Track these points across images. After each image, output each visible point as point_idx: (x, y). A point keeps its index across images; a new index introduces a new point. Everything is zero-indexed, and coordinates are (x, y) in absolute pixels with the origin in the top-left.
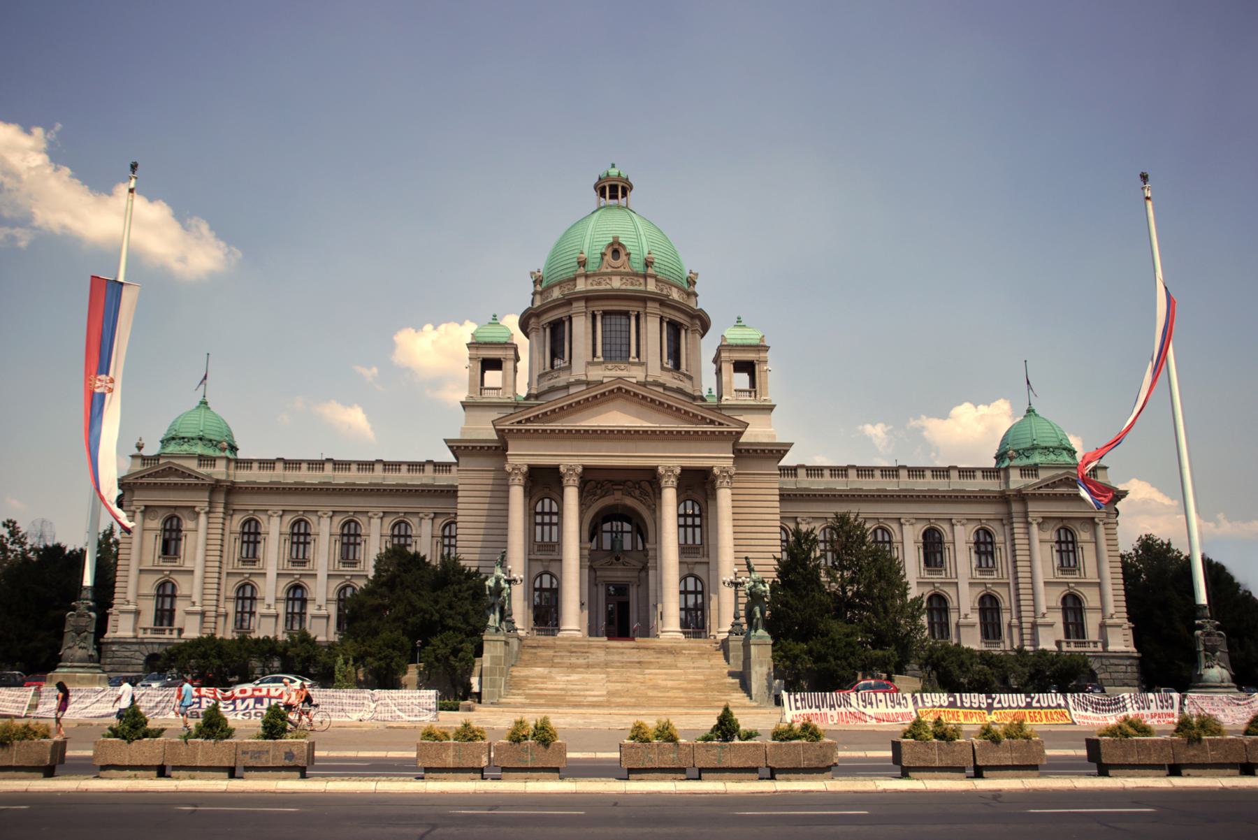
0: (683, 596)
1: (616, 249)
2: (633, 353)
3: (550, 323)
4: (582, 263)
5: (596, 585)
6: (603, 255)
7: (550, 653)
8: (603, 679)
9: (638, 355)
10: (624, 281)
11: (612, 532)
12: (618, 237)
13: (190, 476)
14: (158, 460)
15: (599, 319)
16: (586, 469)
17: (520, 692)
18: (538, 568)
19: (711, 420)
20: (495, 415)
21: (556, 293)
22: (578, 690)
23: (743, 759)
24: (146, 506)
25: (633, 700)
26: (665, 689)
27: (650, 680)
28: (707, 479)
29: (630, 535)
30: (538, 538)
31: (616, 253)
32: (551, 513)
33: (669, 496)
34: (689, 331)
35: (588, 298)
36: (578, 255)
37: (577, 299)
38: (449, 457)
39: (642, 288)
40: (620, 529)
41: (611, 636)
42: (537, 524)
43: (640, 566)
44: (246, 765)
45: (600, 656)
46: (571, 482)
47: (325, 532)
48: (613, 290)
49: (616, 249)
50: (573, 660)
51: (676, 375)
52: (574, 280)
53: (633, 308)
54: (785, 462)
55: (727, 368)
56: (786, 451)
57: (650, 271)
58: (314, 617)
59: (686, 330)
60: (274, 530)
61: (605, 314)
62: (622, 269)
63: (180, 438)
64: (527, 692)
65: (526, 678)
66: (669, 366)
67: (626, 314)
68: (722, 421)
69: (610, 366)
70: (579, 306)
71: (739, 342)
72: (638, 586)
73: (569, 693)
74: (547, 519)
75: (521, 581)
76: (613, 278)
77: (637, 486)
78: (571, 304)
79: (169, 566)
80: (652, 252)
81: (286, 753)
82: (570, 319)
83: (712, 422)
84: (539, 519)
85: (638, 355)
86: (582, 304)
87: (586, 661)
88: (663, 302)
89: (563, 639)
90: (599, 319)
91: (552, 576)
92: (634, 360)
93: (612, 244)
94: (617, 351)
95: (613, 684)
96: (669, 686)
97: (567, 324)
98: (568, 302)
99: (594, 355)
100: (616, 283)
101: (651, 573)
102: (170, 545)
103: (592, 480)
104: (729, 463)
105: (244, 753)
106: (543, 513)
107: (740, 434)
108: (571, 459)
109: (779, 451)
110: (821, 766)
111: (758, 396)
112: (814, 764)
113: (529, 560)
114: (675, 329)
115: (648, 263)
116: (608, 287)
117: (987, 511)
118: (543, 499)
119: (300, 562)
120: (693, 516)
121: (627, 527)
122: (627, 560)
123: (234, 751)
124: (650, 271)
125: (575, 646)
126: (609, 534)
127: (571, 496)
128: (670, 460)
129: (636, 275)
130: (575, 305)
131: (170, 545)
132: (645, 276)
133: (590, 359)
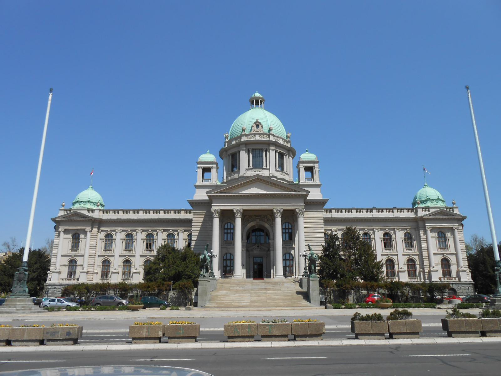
0: (284, 261)
1: (257, 124)
2: (265, 164)
3: (231, 154)
5: (249, 257)
6: (252, 126)
7: (229, 285)
8: (249, 296)
9: (266, 166)
10: (261, 136)
11: (256, 236)
12: (258, 120)
14: (71, 211)
16: (245, 211)
17: (214, 302)
18: (225, 251)
19: (294, 190)
20: (207, 190)
22: (239, 300)
23: (281, 331)
25: (261, 304)
26: (274, 299)
27: (269, 295)
28: (294, 214)
29: (263, 237)
30: (225, 239)
31: (257, 126)
32: (230, 229)
33: (279, 221)
34: (287, 156)
35: (246, 144)
36: (242, 127)
38: (190, 208)
39: (268, 139)
40: (259, 234)
41: (255, 278)
42: (225, 233)
43: (267, 249)
44: (48, 339)
45: (249, 287)
46: (238, 216)
47: (140, 237)
48: (256, 140)
49: (257, 124)
50: (238, 288)
51: (282, 173)
52: (240, 137)
53: (264, 147)
54: (326, 207)
55: (302, 170)
56: (326, 202)
57: (271, 132)
58: (134, 273)
59: (286, 156)
61: (253, 150)
62: (260, 132)
64: (217, 301)
65: (217, 296)
66: (279, 170)
68: (298, 190)
69: (255, 170)
71: (307, 160)
72: (267, 258)
73: (234, 302)
74: (229, 231)
75: (217, 256)
76: (256, 135)
77: (266, 217)
78: (240, 146)
79: (74, 253)
80: (272, 125)
81: (67, 332)
83: (295, 191)
84: (226, 231)
85: (266, 166)
86: (244, 146)
87: (243, 288)
88: (276, 144)
89: (234, 280)
90: (251, 151)
91: (231, 254)
92: (265, 168)
93: (255, 123)
94: (257, 163)
95: (253, 298)
96: (276, 298)
97: (238, 154)
100: (258, 138)
101: (271, 252)
102: (75, 245)
103: (247, 216)
104: (303, 207)
105: (47, 333)
106: (227, 229)
107: (307, 196)
108: (237, 207)
109: (323, 202)
110: (317, 333)
111: (315, 181)
112: (314, 333)
113: (221, 248)
114: (281, 156)
115: (270, 130)
116: (254, 139)
118: (227, 223)
120: (289, 229)
121: (262, 234)
122: (262, 247)
123: (42, 332)
124: (271, 132)
125: (239, 282)
126: (254, 237)
127: (238, 222)
128: (278, 207)
129: (266, 134)
130: (241, 146)
131: (75, 245)
132: (269, 135)
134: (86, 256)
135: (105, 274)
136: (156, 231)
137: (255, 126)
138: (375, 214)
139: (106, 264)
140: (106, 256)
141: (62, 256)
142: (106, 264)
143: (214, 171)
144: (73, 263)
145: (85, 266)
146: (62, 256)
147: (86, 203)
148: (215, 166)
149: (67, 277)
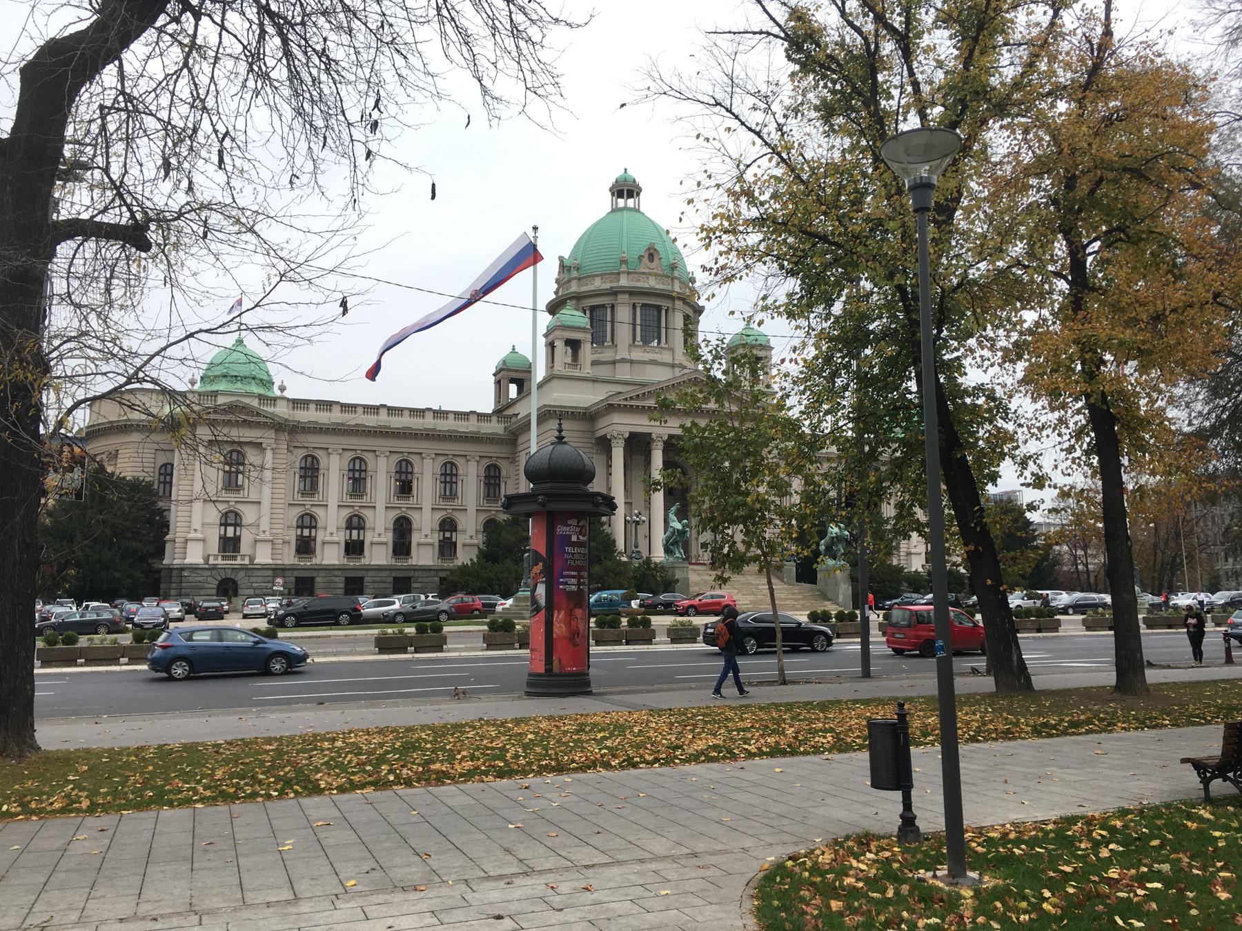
4: (624, 262)
15: (638, 310)
21: (598, 284)
35: (632, 292)
37: (623, 292)
53: (665, 304)
61: (643, 305)
62: (655, 271)
67: (659, 308)
82: (613, 307)
90: (638, 310)
93: (649, 249)
98: (614, 293)
99: (634, 340)
100: (652, 283)
116: (646, 285)
117: (493, 450)
130: (619, 296)
133: (631, 342)
134: (266, 504)
135: (305, 547)
137: (646, 257)
139: (308, 522)
142: (308, 522)
144: (231, 519)
145: (265, 525)
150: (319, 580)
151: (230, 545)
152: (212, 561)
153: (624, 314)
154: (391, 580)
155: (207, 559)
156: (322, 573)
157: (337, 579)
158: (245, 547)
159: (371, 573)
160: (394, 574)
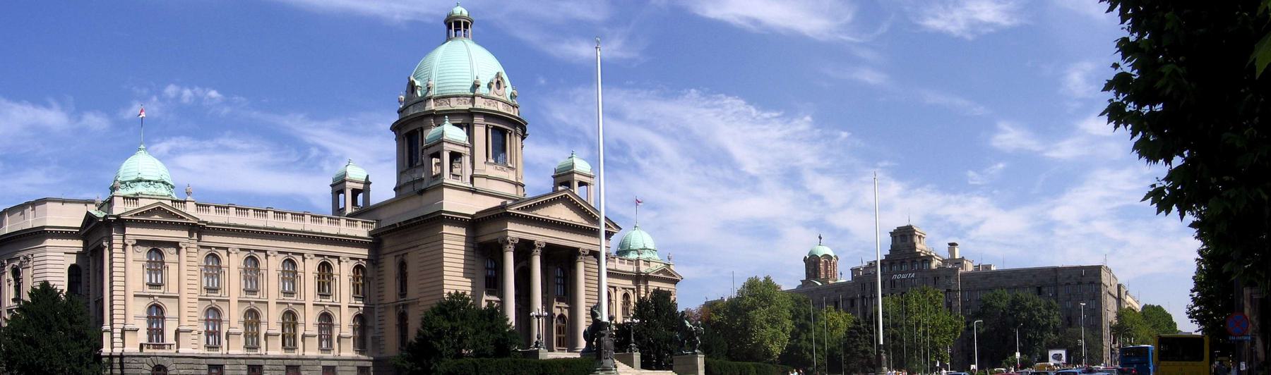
13: (182, 218)
15: (490, 130)
21: (456, 105)
24: (137, 240)
31: (498, 83)
35: (488, 115)
60: (234, 264)
62: (501, 98)
63: (146, 181)
70: (477, 120)
90: (490, 130)
98: (471, 114)
100: (501, 108)
116: (496, 109)
119: (253, 291)
134: (184, 300)
136: (176, 245)
138: (271, 221)
140: (157, 296)
141: (135, 296)
143: (466, 160)
146: (135, 296)
147: (135, 184)
148: (468, 150)
149: (149, 341)
150: (227, 367)
151: (156, 333)
152: (145, 350)
153: (480, 132)
154: (284, 368)
155: (141, 346)
156: (228, 362)
157: (241, 367)
158: (169, 337)
159: (269, 362)
160: (287, 362)
